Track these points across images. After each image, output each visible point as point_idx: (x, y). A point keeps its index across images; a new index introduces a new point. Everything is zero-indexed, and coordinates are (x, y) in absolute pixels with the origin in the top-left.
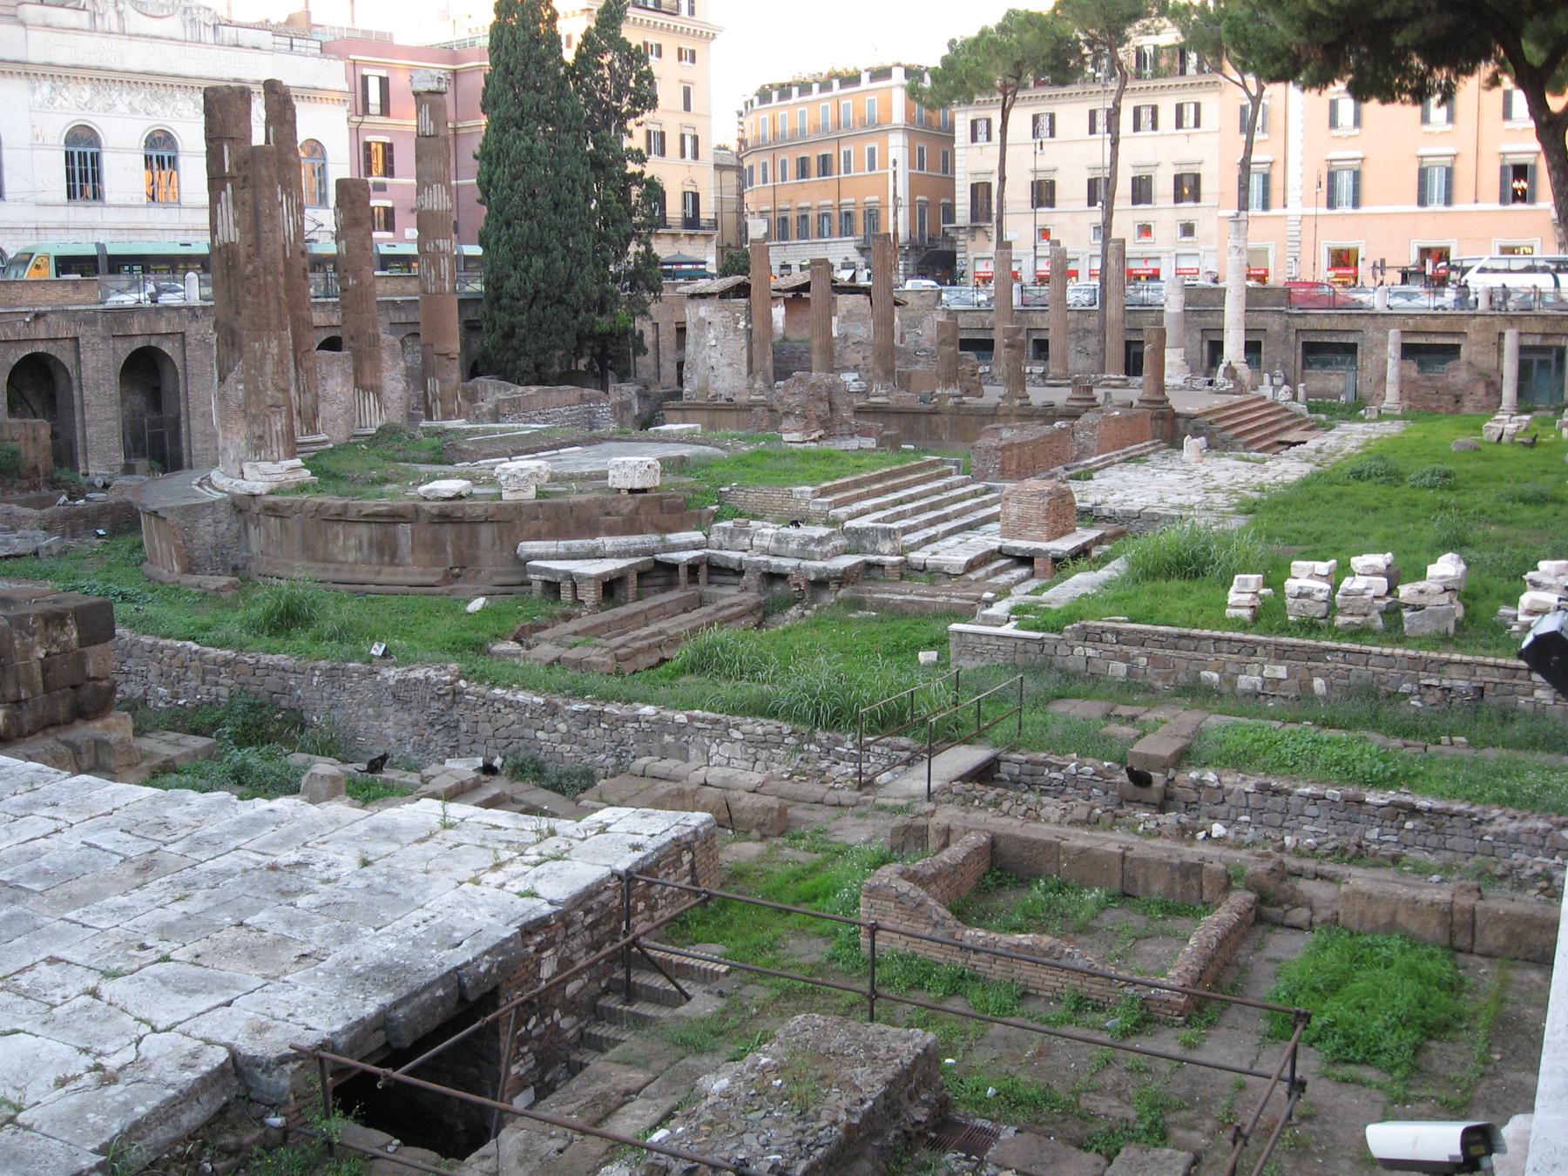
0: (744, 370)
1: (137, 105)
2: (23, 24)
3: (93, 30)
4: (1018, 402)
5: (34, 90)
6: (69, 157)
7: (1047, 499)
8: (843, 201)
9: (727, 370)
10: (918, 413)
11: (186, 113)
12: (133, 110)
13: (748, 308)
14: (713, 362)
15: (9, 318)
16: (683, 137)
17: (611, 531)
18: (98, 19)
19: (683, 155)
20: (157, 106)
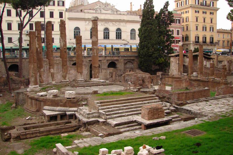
0: (178, 71)
1: (102, 24)
2: (85, 13)
3: (96, 13)
4: (224, 81)
5: (86, 22)
7: (148, 110)
9: (175, 70)
10: (205, 82)
11: (111, 25)
12: (102, 25)
13: (179, 59)
14: (173, 69)
17: (61, 106)
18: (97, 11)
20: (106, 24)
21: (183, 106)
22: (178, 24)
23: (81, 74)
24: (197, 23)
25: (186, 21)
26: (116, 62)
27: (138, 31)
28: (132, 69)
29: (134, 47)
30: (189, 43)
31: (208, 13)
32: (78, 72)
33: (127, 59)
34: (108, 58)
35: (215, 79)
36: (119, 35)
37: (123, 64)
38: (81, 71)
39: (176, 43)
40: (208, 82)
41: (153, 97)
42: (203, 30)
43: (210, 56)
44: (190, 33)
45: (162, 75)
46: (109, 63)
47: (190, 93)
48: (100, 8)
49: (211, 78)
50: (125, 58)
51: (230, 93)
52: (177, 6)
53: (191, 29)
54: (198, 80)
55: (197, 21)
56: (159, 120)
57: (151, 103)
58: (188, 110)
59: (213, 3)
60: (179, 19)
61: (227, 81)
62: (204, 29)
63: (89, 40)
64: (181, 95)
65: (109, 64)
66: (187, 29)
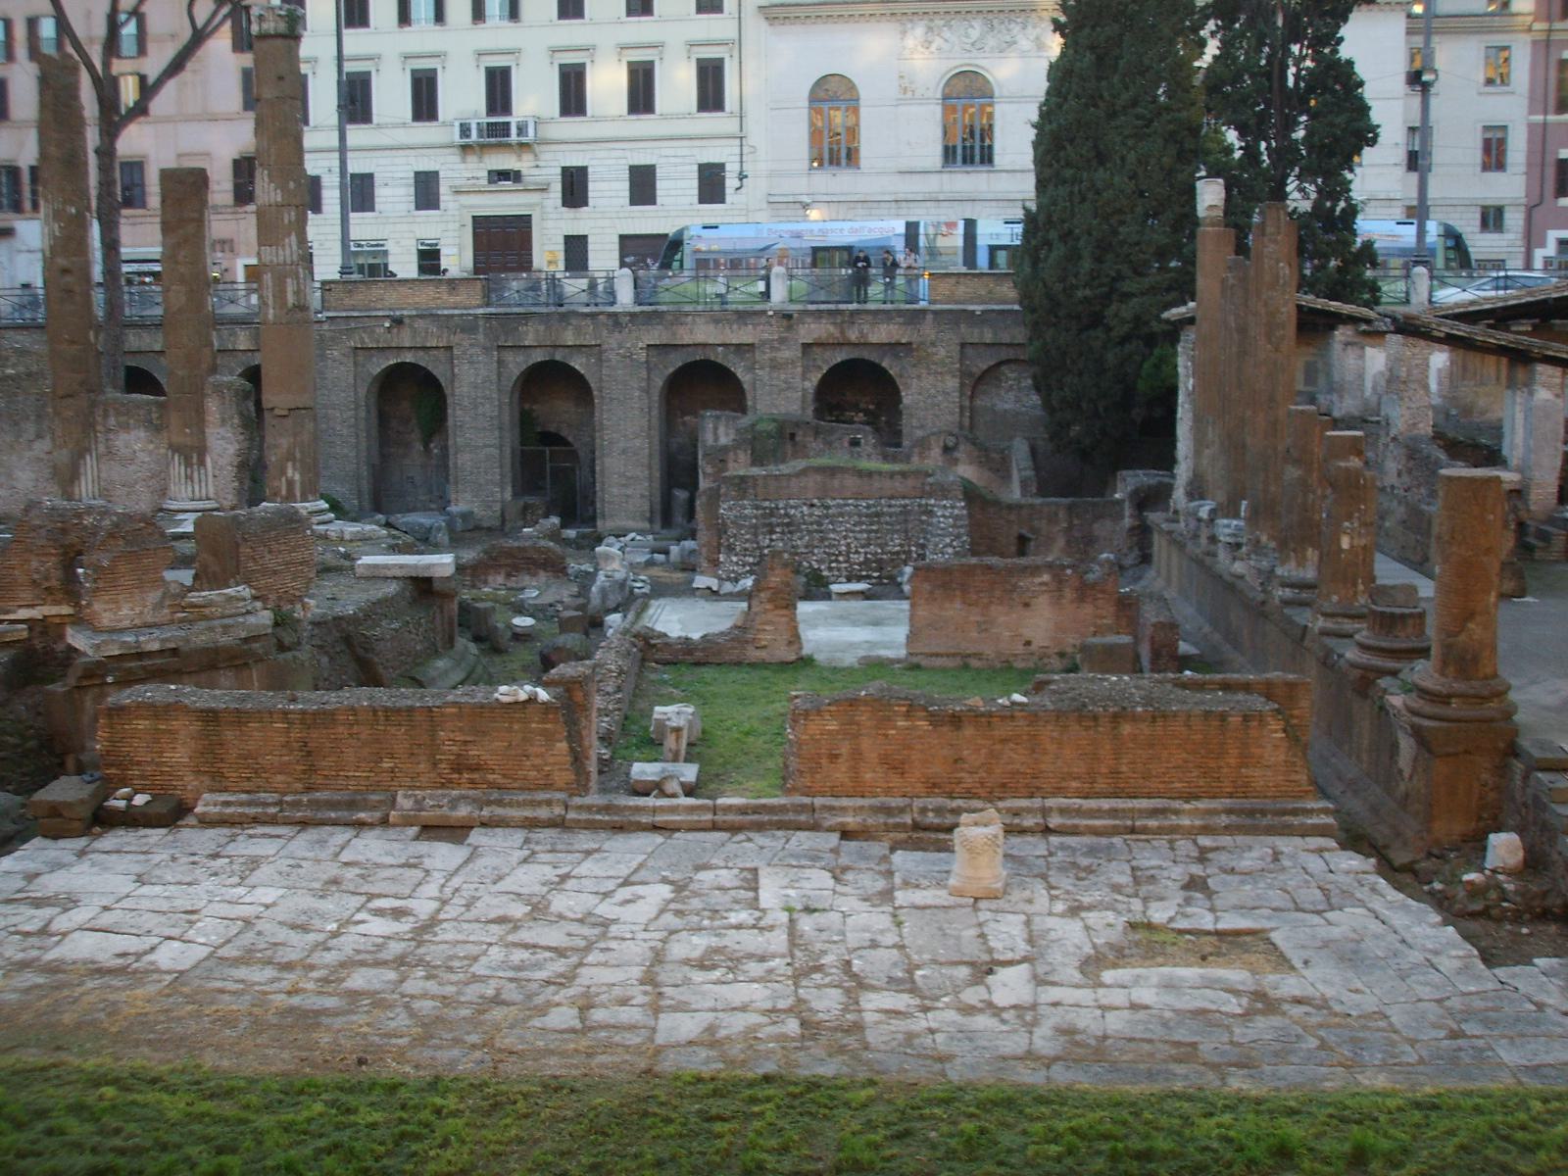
5: (904, 33)
15: (368, 323)
23: (188, 464)
26: (884, 364)
29: (999, 230)
32: (175, 448)
33: (988, 337)
34: (811, 331)
37: (952, 383)
38: (189, 441)
50: (973, 335)
51: (932, 787)
63: (934, 178)
64: (143, 724)
65: (825, 376)
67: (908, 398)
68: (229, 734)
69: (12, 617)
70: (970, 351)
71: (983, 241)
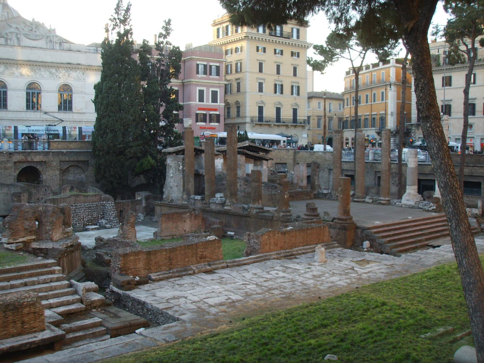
0: (182, 189)
3: (6, 45)
4: (282, 214)
6: (28, 94)
8: (373, 113)
11: (45, 76)
13: (183, 159)
14: (171, 184)
16: (292, 87)
18: (9, 41)
19: (292, 94)
21: (130, 290)
22: (214, 76)
24: (261, 76)
25: (237, 71)
27: (94, 91)
28: (81, 186)
30: (243, 121)
31: (287, 52)
33: (67, 159)
34: (16, 158)
35: (266, 209)
36: (33, 100)
37: (57, 172)
39: (210, 122)
40: (247, 216)
41: (46, 266)
42: (275, 92)
43: (267, 151)
44: (245, 98)
45: (147, 198)
46: (20, 169)
47: (160, 251)
48: (17, 34)
49: (254, 207)
51: (281, 248)
52: (218, 36)
53: (248, 90)
54: (227, 213)
55: (261, 70)
56: (24, 339)
57: (33, 283)
58: (139, 302)
59: (298, 31)
60: (218, 65)
61: (288, 214)
62: (278, 89)
64: (132, 258)
65: (20, 172)
66: (239, 90)
67: (44, 177)
68: (152, 257)
69: (17, 241)
70: (62, 163)
71: (20, 132)
